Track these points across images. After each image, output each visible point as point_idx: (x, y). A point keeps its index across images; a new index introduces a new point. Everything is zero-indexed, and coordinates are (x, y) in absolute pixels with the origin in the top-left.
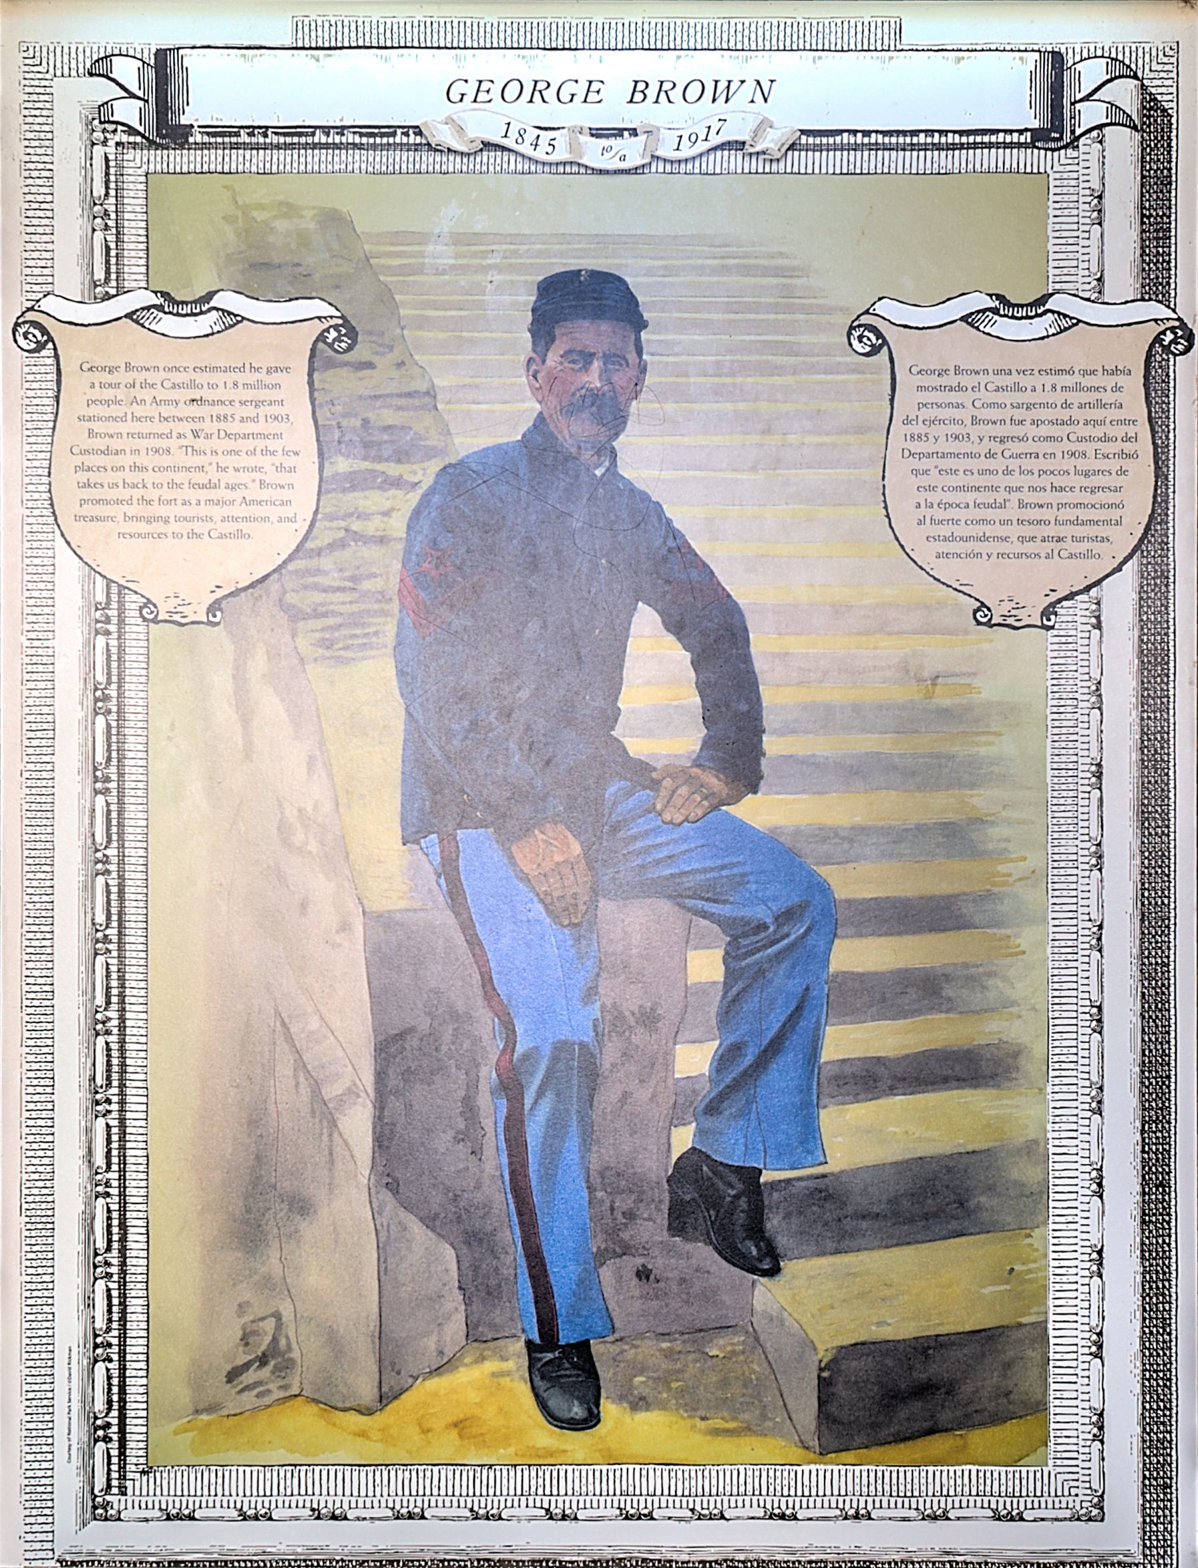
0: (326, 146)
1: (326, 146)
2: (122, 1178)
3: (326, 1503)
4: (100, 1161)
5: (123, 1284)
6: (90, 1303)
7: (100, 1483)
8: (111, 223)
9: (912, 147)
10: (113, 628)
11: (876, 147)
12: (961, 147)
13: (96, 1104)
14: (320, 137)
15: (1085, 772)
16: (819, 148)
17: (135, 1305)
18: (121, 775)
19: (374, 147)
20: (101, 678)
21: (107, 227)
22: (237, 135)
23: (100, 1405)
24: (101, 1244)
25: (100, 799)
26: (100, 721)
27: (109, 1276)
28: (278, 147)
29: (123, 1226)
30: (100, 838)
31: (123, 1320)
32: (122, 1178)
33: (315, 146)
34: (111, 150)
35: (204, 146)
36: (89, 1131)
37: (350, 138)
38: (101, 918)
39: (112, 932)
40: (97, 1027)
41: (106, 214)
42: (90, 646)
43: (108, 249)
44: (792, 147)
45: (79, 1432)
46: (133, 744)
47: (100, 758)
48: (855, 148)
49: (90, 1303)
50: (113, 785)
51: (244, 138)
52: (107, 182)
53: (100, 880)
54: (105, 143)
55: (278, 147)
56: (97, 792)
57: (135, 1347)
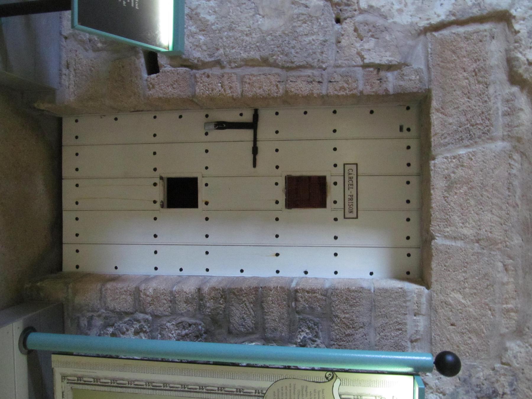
4: (136, 383)
5: (110, 386)
6: (105, 378)
7: (69, 378)
10: (257, 394)
13: (148, 383)
17: (106, 389)
18: (222, 394)
20: (245, 391)
23: (85, 379)
24: (118, 382)
25: (216, 389)
26: (235, 390)
29: (122, 387)
30: (208, 388)
31: (102, 386)
36: (142, 381)
38: (190, 387)
39: (186, 389)
40: (165, 384)
47: (226, 389)
49: (105, 378)
50: (220, 392)
53: (198, 387)
56: (218, 388)
57: (97, 388)
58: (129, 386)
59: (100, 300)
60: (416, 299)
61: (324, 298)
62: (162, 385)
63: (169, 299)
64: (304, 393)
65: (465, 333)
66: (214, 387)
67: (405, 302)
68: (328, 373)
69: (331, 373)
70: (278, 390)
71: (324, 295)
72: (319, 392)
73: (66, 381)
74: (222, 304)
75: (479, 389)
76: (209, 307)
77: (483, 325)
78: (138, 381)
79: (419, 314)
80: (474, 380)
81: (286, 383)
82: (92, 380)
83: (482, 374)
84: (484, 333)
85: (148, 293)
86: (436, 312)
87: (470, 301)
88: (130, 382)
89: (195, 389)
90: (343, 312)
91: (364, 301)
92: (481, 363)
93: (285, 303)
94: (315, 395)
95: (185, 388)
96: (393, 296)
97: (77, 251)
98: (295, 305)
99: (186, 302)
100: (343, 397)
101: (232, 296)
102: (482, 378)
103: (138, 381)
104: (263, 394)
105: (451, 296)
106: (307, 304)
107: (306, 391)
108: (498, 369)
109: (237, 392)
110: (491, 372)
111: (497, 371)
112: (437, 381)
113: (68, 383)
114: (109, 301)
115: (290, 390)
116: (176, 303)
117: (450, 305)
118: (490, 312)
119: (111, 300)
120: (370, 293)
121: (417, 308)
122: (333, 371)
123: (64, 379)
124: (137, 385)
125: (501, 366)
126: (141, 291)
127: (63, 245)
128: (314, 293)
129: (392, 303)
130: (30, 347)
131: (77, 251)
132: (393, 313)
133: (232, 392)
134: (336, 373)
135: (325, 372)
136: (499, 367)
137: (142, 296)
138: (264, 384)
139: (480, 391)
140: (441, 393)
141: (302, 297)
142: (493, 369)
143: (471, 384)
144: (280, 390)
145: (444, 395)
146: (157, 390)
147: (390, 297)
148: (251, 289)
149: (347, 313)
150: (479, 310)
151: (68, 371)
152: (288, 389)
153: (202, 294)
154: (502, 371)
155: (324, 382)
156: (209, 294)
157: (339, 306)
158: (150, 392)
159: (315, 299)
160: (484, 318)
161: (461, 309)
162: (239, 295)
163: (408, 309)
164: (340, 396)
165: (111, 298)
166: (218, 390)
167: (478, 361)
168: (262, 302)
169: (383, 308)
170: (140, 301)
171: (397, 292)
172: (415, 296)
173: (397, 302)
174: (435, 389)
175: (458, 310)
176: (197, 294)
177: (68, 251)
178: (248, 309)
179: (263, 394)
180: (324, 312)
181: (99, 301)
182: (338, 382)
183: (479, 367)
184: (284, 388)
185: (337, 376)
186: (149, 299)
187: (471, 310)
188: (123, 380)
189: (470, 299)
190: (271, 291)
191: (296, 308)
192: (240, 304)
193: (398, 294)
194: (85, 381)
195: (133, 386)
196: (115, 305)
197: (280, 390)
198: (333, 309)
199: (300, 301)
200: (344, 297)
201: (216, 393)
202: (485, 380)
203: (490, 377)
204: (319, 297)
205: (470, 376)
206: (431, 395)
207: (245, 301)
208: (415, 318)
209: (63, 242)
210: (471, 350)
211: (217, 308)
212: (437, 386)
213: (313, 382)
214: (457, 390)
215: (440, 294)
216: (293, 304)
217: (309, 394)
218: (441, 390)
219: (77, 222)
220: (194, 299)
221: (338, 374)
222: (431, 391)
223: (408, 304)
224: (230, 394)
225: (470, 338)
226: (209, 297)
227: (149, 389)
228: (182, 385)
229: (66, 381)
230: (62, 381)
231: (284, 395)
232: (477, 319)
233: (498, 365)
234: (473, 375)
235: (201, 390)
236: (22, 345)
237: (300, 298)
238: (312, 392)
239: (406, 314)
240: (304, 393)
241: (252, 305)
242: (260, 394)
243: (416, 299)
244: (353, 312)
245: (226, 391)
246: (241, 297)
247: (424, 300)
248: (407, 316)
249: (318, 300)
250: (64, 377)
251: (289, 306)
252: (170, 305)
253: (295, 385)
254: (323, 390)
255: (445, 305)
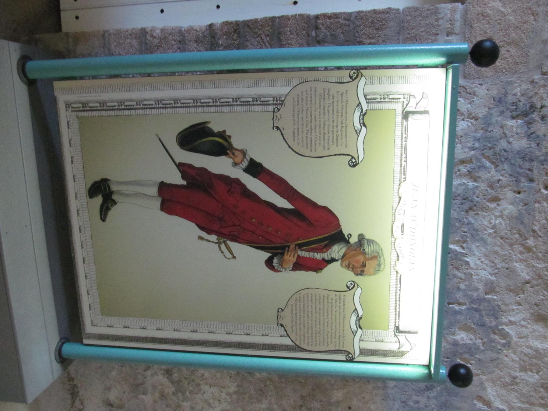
0: (401, 157)
1: (401, 157)
2: (141, 109)
3: (75, 160)
4: (145, 103)
6: (112, 101)
7: (74, 106)
8: (382, 100)
9: (396, 301)
10: (275, 102)
11: (396, 292)
12: (396, 312)
13: (158, 101)
14: (404, 156)
15: (249, 332)
16: (397, 279)
17: (113, 113)
18: (238, 105)
19: (401, 170)
20: (262, 99)
21: (381, 99)
22: (405, 134)
23: (90, 105)
24: (126, 104)
25: (231, 100)
27: (119, 106)
28: (402, 145)
30: (222, 100)
31: (109, 110)
32: (141, 109)
33: (401, 154)
34: (402, 100)
35: (402, 125)
37: (404, 163)
38: (202, 101)
39: (199, 104)
40: (176, 101)
41: (384, 99)
42: (270, 96)
43: (375, 99)
44: (397, 272)
45: (84, 99)
46: (246, 108)
47: (242, 100)
48: (396, 288)
49: (112, 101)
50: (235, 103)
51: (404, 136)
52: (393, 99)
53: (211, 101)
54: (404, 98)
55: (402, 145)
56: (233, 99)
57: (104, 113)
58: (138, 106)
59: (103, 48)
60: (449, 16)
61: (348, 23)
62: (173, 102)
63: (178, 39)
64: (327, 96)
65: (503, 46)
66: (228, 98)
67: (437, 20)
68: (353, 72)
69: (356, 72)
70: (298, 95)
71: (348, 20)
72: (342, 94)
73: (70, 109)
74: (235, 40)
75: (515, 107)
76: (222, 45)
77: (524, 33)
78: (146, 100)
79: (452, 34)
80: (510, 99)
81: (306, 86)
82: (98, 105)
83: (519, 89)
84: (524, 43)
85: (155, 35)
86: (472, 27)
87: (510, 8)
88: (138, 102)
89: (209, 103)
90: (368, 37)
91: (392, 23)
92: (520, 77)
93: (304, 32)
94: (338, 98)
95: (197, 102)
96: (424, 14)
97: (77, 18)
98: (316, 33)
99: (196, 42)
100: (368, 97)
101: (247, 29)
102: (519, 94)
103: (146, 100)
104: (281, 101)
105: (489, 5)
106: (329, 32)
107: (328, 94)
108: (538, 81)
109: (253, 101)
110: (530, 86)
111: (537, 83)
112: (469, 106)
113: (72, 111)
114: (113, 48)
115: (311, 94)
116: (186, 43)
117: (488, 16)
118: (532, 17)
119: (115, 46)
120: (399, 13)
121: (450, 26)
122: (358, 69)
123: (69, 107)
124: (146, 105)
125: (541, 76)
126: (147, 33)
127: (62, 12)
128: (337, 18)
129: (423, 22)
130: (31, 76)
131: (77, 18)
132: (423, 34)
133: (248, 102)
134: (361, 71)
135: (349, 71)
136: (538, 79)
137: (149, 38)
138: (283, 90)
139: (516, 109)
140: (473, 118)
141: (323, 25)
142: (532, 82)
143: (506, 103)
144: (300, 95)
145: (476, 120)
146: (167, 108)
147: (421, 15)
148: (267, 20)
149: (373, 38)
150: (519, 17)
151: (72, 98)
152: (309, 92)
153: (214, 30)
154: (542, 83)
155: (348, 82)
156: (221, 30)
157: (363, 31)
158: (162, 111)
159: (338, 25)
160: (525, 25)
161: (499, 20)
162: (254, 28)
163: (440, 28)
164: (365, 96)
165: (115, 44)
166: (233, 101)
167: (517, 75)
168: (280, 33)
169: (413, 29)
170: (146, 44)
171: (428, 10)
172: (449, 12)
173: (428, 21)
174: (466, 115)
175: (496, 21)
176: (208, 32)
177: (67, 18)
178: (264, 43)
179: (281, 101)
180: (348, 39)
181: (102, 50)
182: (363, 80)
183: (516, 83)
184: (304, 93)
185: (362, 75)
186: (156, 41)
187: (511, 18)
188: (131, 100)
189: (511, 5)
190: (289, 20)
191: (316, 37)
192: (255, 38)
193: (429, 12)
194: (91, 107)
195: (142, 106)
196: (120, 51)
197: (300, 95)
198: (357, 34)
199: (320, 29)
200: (370, 20)
201: (231, 105)
202: (523, 95)
203: (527, 91)
204: (342, 22)
205: (506, 94)
206: (462, 122)
207: (261, 34)
208: (447, 38)
209: (61, 9)
210: (508, 65)
211: (230, 44)
212: (468, 111)
213: (335, 83)
214: (491, 112)
215: (476, 6)
216: (313, 33)
217: (331, 97)
218: (474, 114)
219: (77, 21)
220: (205, 36)
221: (363, 71)
222: (462, 117)
223: (441, 22)
224: (246, 105)
225: (508, 51)
226: (221, 33)
227: (159, 108)
228: (194, 100)
229: (70, 109)
230: (66, 110)
231: (304, 101)
232: (517, 27)
233: (537, 77)
234: (509, 92)
235: (215, 104)
236: (21, 72)
237: (321, 26)
238: (335, 95)
239: (437, 34)
240: (327, 96)
241: (268, 39)
242: (279, 102)
243: (449, 16)
244: (379, 36)
245: (241, 102)
246: (257, 30)
247: (458, 16)
248: (438, 36)
249: (342, 25)
250: (68, 105)
251: (309, 36)
252: (180, 46)
253: (316, 88)
254: (347, 91)
255: (482, 17)
